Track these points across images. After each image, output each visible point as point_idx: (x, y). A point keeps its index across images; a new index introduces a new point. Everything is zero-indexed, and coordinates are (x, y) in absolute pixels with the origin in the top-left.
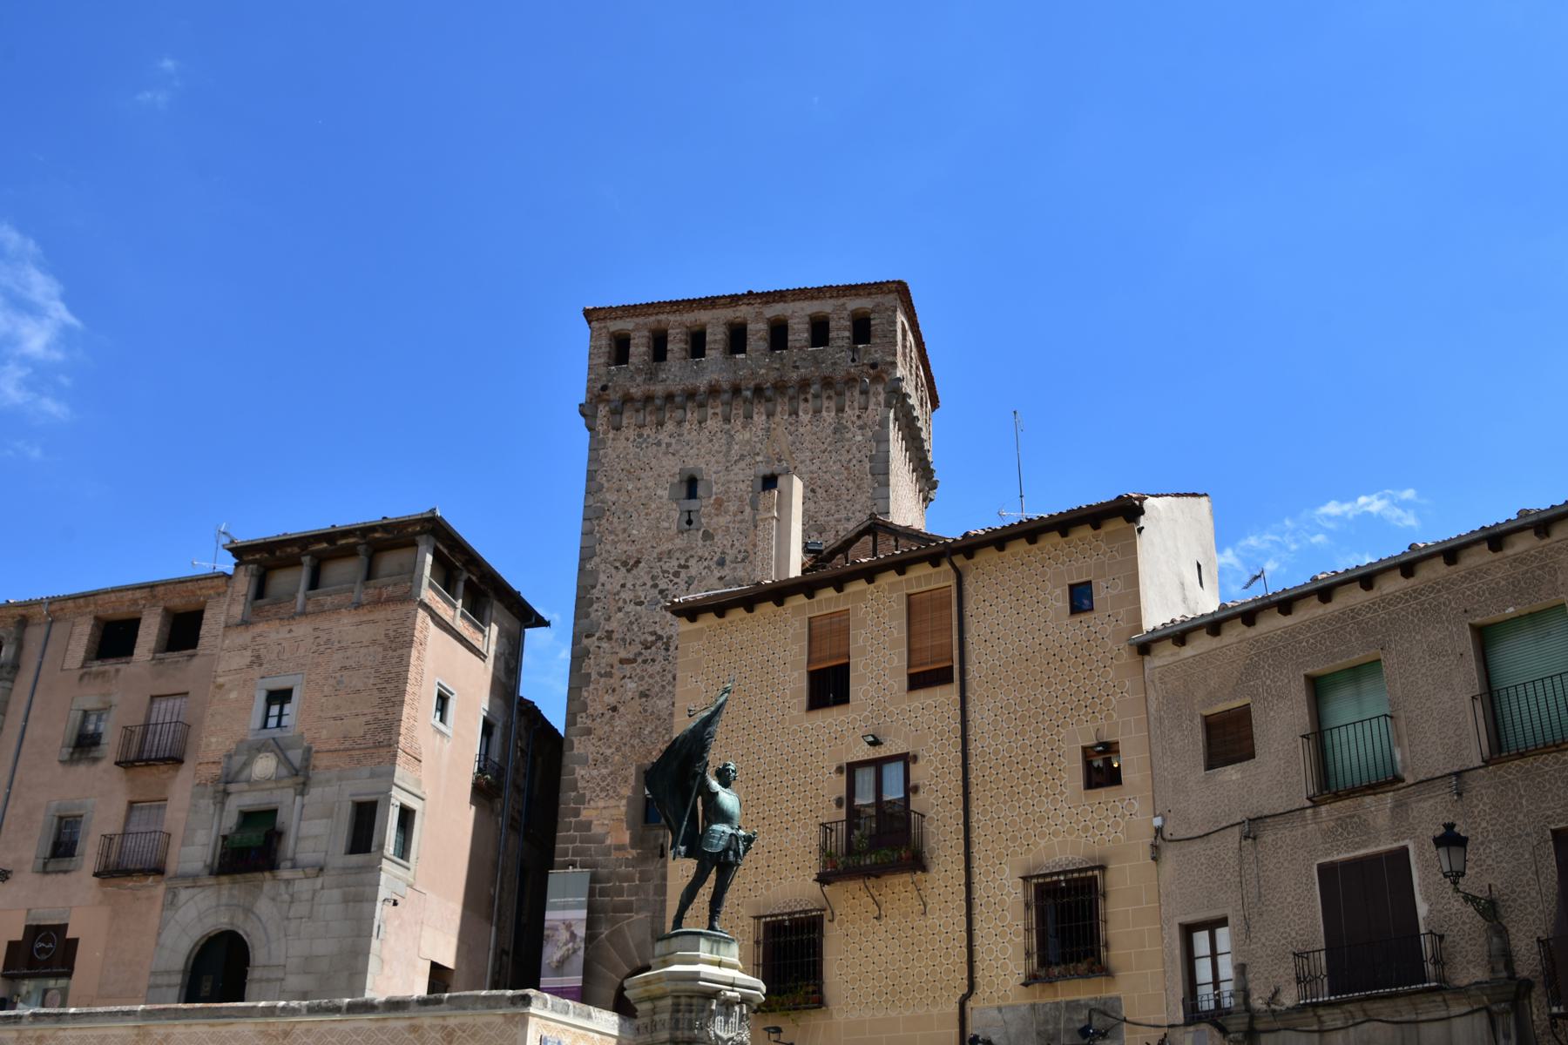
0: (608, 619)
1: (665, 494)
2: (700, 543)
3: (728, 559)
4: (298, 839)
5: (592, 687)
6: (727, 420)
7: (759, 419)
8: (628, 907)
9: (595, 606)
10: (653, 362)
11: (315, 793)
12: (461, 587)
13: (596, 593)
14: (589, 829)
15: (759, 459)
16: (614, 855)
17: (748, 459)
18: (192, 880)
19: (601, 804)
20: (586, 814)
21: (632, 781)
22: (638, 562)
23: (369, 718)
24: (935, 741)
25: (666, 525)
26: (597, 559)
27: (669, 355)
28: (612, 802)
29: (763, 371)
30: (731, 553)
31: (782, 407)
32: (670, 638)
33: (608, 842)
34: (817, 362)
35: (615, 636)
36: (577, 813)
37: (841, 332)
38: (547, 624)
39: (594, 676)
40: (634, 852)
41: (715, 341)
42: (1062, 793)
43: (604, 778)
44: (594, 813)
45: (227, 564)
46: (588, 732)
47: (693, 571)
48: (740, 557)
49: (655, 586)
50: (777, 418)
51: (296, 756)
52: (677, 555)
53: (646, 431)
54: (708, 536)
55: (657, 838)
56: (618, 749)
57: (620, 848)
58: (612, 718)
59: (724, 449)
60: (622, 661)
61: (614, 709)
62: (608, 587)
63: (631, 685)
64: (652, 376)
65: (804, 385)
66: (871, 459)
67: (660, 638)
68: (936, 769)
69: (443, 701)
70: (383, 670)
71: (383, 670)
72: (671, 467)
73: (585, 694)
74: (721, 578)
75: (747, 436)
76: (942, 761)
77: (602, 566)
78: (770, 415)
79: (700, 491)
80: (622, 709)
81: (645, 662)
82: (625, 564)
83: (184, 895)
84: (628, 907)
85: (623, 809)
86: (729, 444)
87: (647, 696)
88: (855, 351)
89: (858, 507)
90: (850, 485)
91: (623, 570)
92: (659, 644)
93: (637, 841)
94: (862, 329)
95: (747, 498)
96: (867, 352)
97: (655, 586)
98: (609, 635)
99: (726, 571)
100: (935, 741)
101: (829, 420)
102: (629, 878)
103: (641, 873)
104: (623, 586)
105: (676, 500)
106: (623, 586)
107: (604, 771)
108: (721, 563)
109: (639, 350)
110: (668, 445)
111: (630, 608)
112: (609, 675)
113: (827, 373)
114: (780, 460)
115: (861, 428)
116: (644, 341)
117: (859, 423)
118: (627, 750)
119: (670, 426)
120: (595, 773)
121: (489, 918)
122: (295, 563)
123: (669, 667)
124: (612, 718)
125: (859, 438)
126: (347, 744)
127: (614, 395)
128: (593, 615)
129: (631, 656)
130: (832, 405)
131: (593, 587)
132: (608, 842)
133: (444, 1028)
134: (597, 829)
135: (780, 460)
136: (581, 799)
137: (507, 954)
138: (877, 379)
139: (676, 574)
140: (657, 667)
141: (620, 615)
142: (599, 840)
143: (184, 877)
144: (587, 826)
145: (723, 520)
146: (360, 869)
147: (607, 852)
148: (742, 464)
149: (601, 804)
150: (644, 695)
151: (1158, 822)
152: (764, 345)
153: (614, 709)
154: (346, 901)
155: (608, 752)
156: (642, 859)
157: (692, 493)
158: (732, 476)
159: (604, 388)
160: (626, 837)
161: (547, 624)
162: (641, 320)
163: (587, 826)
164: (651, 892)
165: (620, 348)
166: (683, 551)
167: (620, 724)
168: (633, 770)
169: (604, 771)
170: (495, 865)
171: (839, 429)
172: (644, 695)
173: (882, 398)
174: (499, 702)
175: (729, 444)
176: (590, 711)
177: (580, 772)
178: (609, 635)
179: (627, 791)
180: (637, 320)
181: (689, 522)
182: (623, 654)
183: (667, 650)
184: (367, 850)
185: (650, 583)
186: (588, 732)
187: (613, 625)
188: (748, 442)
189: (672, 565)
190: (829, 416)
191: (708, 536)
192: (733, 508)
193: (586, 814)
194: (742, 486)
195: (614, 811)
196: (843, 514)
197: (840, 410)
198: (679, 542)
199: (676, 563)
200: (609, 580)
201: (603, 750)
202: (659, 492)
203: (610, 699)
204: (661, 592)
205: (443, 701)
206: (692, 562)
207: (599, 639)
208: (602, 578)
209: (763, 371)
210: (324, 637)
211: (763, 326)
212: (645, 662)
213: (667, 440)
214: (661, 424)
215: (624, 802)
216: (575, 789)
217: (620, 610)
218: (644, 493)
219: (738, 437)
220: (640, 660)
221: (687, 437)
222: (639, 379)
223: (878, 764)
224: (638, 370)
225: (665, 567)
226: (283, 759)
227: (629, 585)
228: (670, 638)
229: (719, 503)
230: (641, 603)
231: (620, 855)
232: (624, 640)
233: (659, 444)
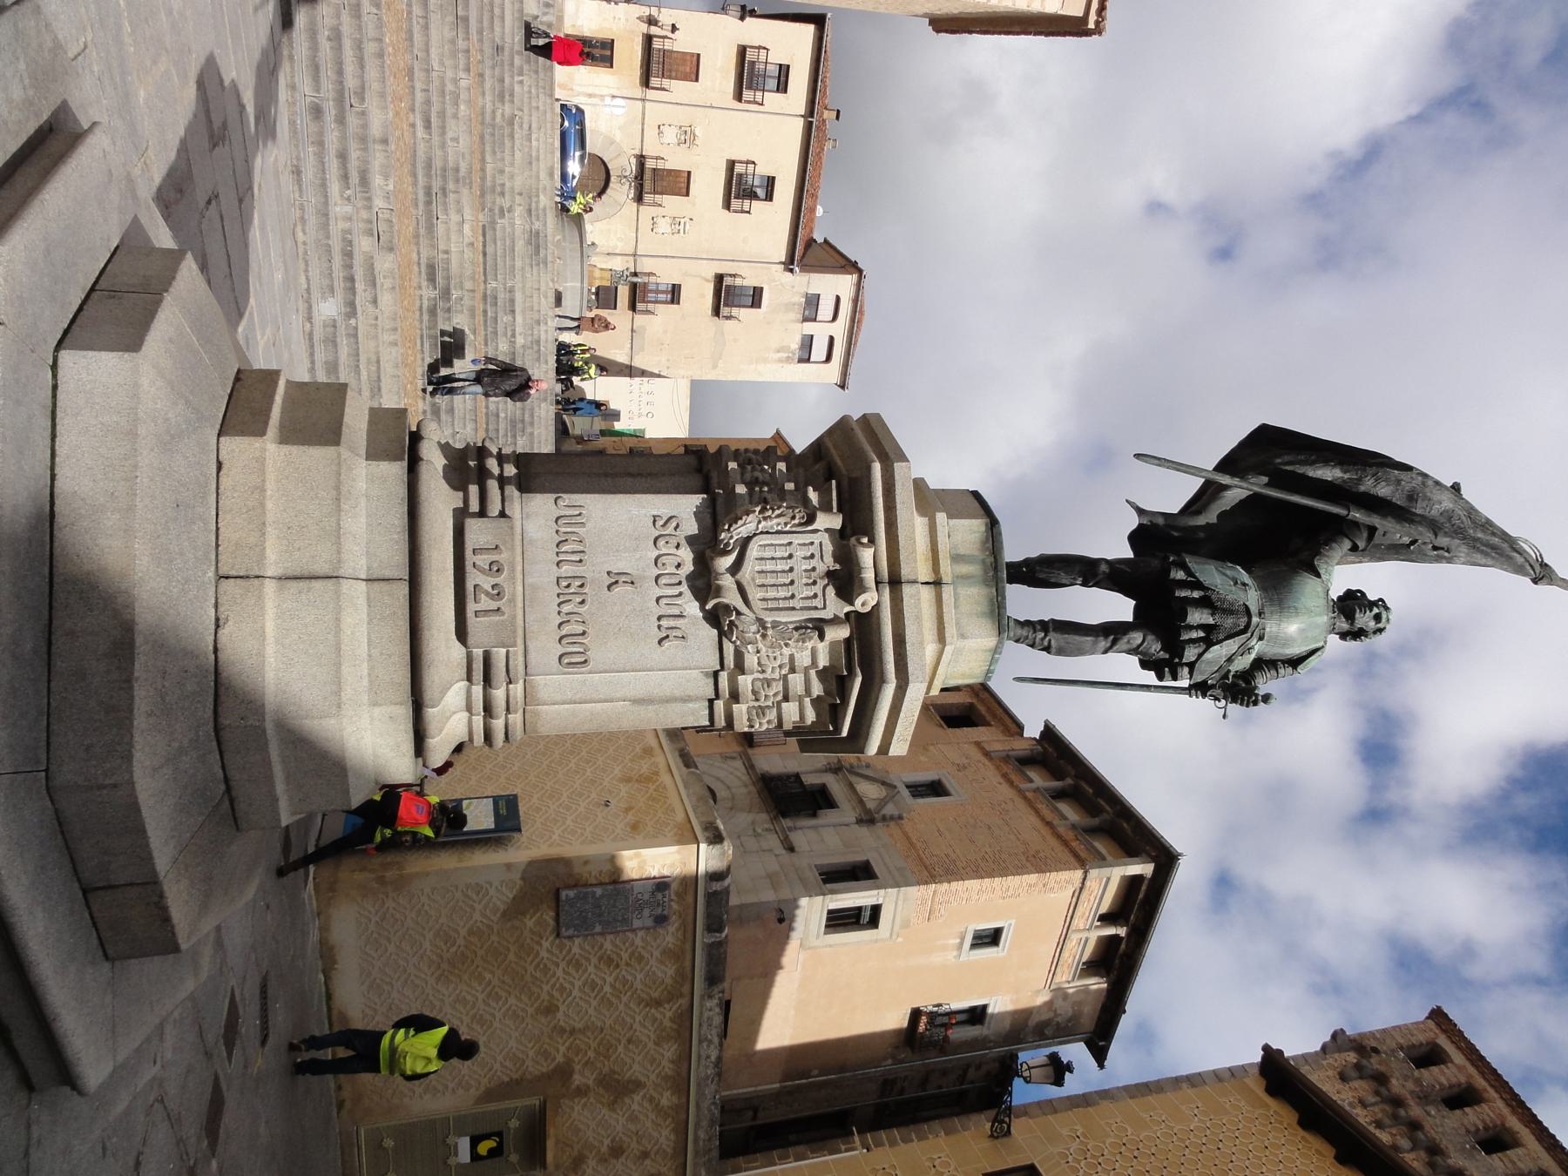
4: (815, 828)
11: (863, 831)
12: (1110, 931)
18: (750, 766)
27: (1458, 1112)
38: (1101, 1066)
45: (1033, 730)
51: (889, 810)
64: (1424, 1098)
69: (992, 938)
83: (738, 764)
109: (1437, 1076)
116: (1454, 1080)
121: (787, 1076)
122: (1057, 774)
127: (1374, 1063)
133: (657, 774)
137: (755, 1118)
143: (749, 760)
146: (803, 880)
154: (770, 876)
159: (1375, 1050)
161: (1101, 1066)
165: (1428, 1057)
170: (842, 1069)
174: (1007, 1024)
184: (825, 881)
205: (992, 938)
222: (1410, 1085)
224: (1418, 1081)
226: (883, 802)
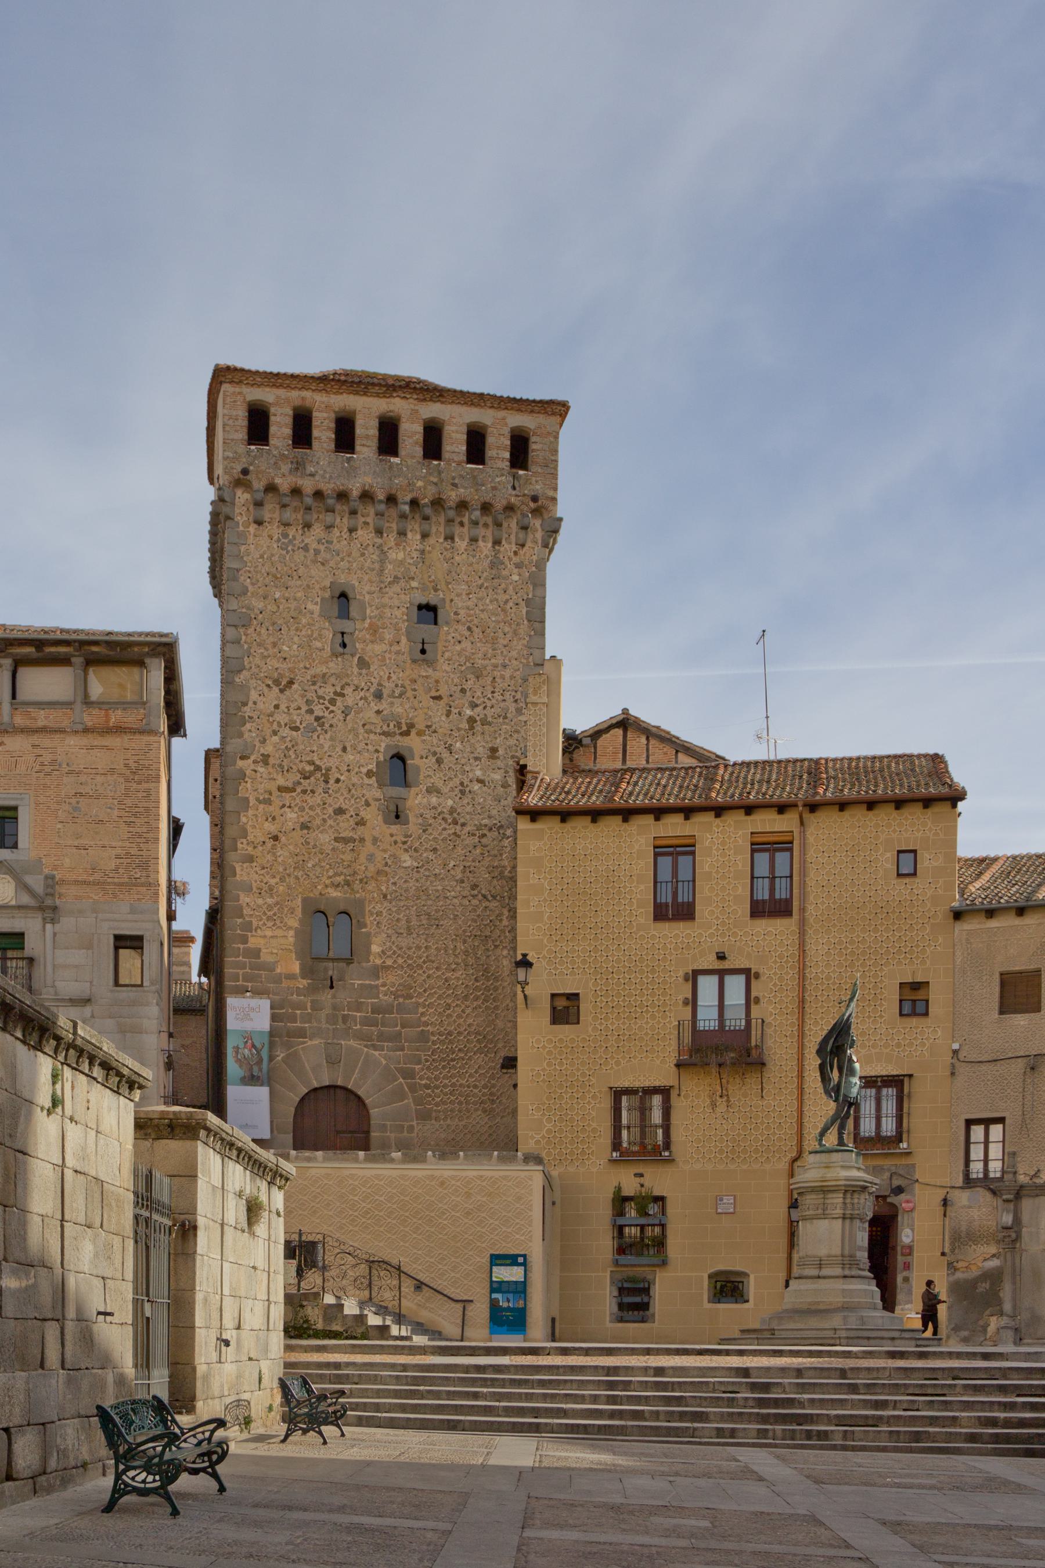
0: (264, 741)
1: (317, 609)
2: (356, 670)
3: (386, 692)
5: (250, 812)
6: (379, 532)
7: (414, 537)
8: (302, 1033)
9: (248, 726)
10: (296, 445)
13: (247, 711)
14: (259, 957)
15: (414, 584)
16: (285, 984)
17: (402, 583)
19: (269, 933)
20: (253, 942)
21: (299, 912)
22: (291, 682)
23: (119, 851)
24: (775, 962)
25: (319, 645)
26: (245, 674)
28: (279, 933)
29: (420, 484)
30: (388, 686)
31: (438, 527)
32: (328, 769)
33: (278, 971)
34: (477, 484)
35: (271, 761)
36: (245, 941)
37: (498, 448)
39: (252, 802)
40: (305, 982)
41: (367, 437)
42: (881, 1016)
43: (270, 907)
44: (262, 941)
46: (250, 859)
47: (350, 701)
48: (397, 692)
49: (310, 711)
50: (432, 540)
52: (333, 680)
53: (291, 532)
54: (363, 663)
55: (326, 969)
56: (282, 880)
57: (291, 977)
58: (274, 847)
59: (377, 566)
60: (280, 789)
61: (276, 838)
62: (260, 706)
63: (291, 815)
65: (462, 505)
66: (528, 602)
67: (318, 768)
68: (775, 985)
70: (129, 802)
71: (129, 802)
72: (321, 578)
73: (244, 819)
74: (378, 712)
75: (401, 556)
76: (781, 979)
77: (253, 683)
78: (425, 536)
79: (354, 612)
80: (283, 839)
81: (304, 792)
82: (277, 682)
84: (302, 1033)
85: (292, 940)
86: (382, 562)
87: (308, 828)
88: (515, 477)
89: (514, 654)
90: (507, 629)
91: (276, 689)
92: (318, 775)
93: (307, 971)
94: (520, 449)
95: (404, 626)
96: (527, 481)
97: (310, 711)
98: (265, 759)
99: (384, 705)
100: (775, 962)
101: (486, 552)
102: (301, 1006)
103: (312, 1002)
104: (277, 707)
105: (328, 618)
106: (277, 707)
107: (269, 901)
108: (378, 696)
110: (317, 552)
111: (286, 732)
112: (268, 802)
113: (487, 498)
114: (436, 590)
115: (518, 566)
117: (516, 559)
118: (292, 881)
119: (317, 530)
120: (260, 901)
123: (329, 801)
124: (274, 847)
125: (515, 578)
126: (97, 876)
128: (246, 736)
129: (290, 785)
130: (489, 533)
131: (245, 704)
132: (278, 971)
134: (265, 957)
135: (436, 590)
136: (248, 927)
138: (537, 512)
139: (333, 702)
140: (317, 799)
141: (275, 739)
142: (270, 968)
144: (256, 953)
145: (379, 648)
147: (278, 980)
148: (396, 588)
149: (269, 933)
150: (304, 826)
151: (956, 1046)
152: (419, 451)
153: (276, 838)
155: (273, 882)
156: (312, 989)
157: (344, 614)
158: (386, 600)
159: (245, 472)
160: (296, 967)
162: (281, 392)
163: (256, 953)
164: (323, 1021)
166: (338, 676)
167: (282, 854)
168: (299, 901)
169: (269, 901)
171: (495, 564)
172: (304, 826)
173: (539, 535)
175: (382, 562)
176: (250, 838)
177: (244, 899)
178: (265, 759)
179: (294, 923)
180: (275, 391)
181: (344, 645)
182: (281, 781)
183: (327, 782)
185: (304, 708)
186: (250, 859)
187: (269, 749)
188: (402, 562)
189: (328, 691)
190: (485, 547)
191: (363, 663)
192: (388, 636)
193: (253, 942)
194: (398, 613)
195: (282, 941)
196: (499, 660)
197: (497, 542)
198: (334, 666)
199: (332, 690)
200: (262, 699)
201: (267, 878)
202: (310, 606)
203: (271, 827)
204: (317, 719)
206: (348, 691)
207: (255, 762)
208: (254, 695)
209: (420, 484)
210: (47, 758)
211: (419, 429)
212: (304, 792)
213: (314, 545)
214: (308, 526)
215: (291, 933)
216: (241, 916)
217: (275, 733)
218: (293, 605)
219: (392, 555)
220: (299, 790)
221: (336, 546)
223: (721, 974)
225: (320, 692)
227: (283, 707)
228: (328, 769)
229: (374, 630)
230: (296, 729)
231: (291, 984)
232: (281, 766)
233: (306, 548)
